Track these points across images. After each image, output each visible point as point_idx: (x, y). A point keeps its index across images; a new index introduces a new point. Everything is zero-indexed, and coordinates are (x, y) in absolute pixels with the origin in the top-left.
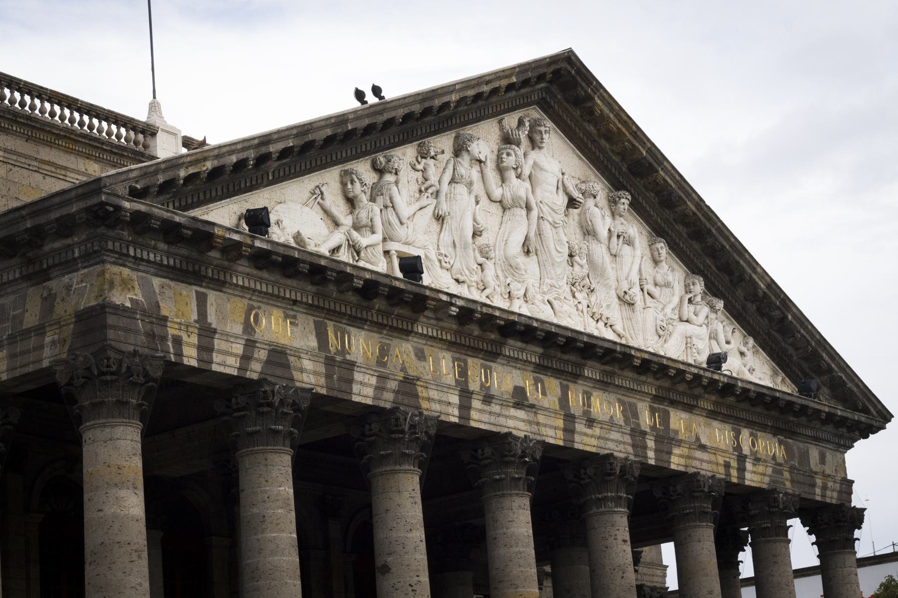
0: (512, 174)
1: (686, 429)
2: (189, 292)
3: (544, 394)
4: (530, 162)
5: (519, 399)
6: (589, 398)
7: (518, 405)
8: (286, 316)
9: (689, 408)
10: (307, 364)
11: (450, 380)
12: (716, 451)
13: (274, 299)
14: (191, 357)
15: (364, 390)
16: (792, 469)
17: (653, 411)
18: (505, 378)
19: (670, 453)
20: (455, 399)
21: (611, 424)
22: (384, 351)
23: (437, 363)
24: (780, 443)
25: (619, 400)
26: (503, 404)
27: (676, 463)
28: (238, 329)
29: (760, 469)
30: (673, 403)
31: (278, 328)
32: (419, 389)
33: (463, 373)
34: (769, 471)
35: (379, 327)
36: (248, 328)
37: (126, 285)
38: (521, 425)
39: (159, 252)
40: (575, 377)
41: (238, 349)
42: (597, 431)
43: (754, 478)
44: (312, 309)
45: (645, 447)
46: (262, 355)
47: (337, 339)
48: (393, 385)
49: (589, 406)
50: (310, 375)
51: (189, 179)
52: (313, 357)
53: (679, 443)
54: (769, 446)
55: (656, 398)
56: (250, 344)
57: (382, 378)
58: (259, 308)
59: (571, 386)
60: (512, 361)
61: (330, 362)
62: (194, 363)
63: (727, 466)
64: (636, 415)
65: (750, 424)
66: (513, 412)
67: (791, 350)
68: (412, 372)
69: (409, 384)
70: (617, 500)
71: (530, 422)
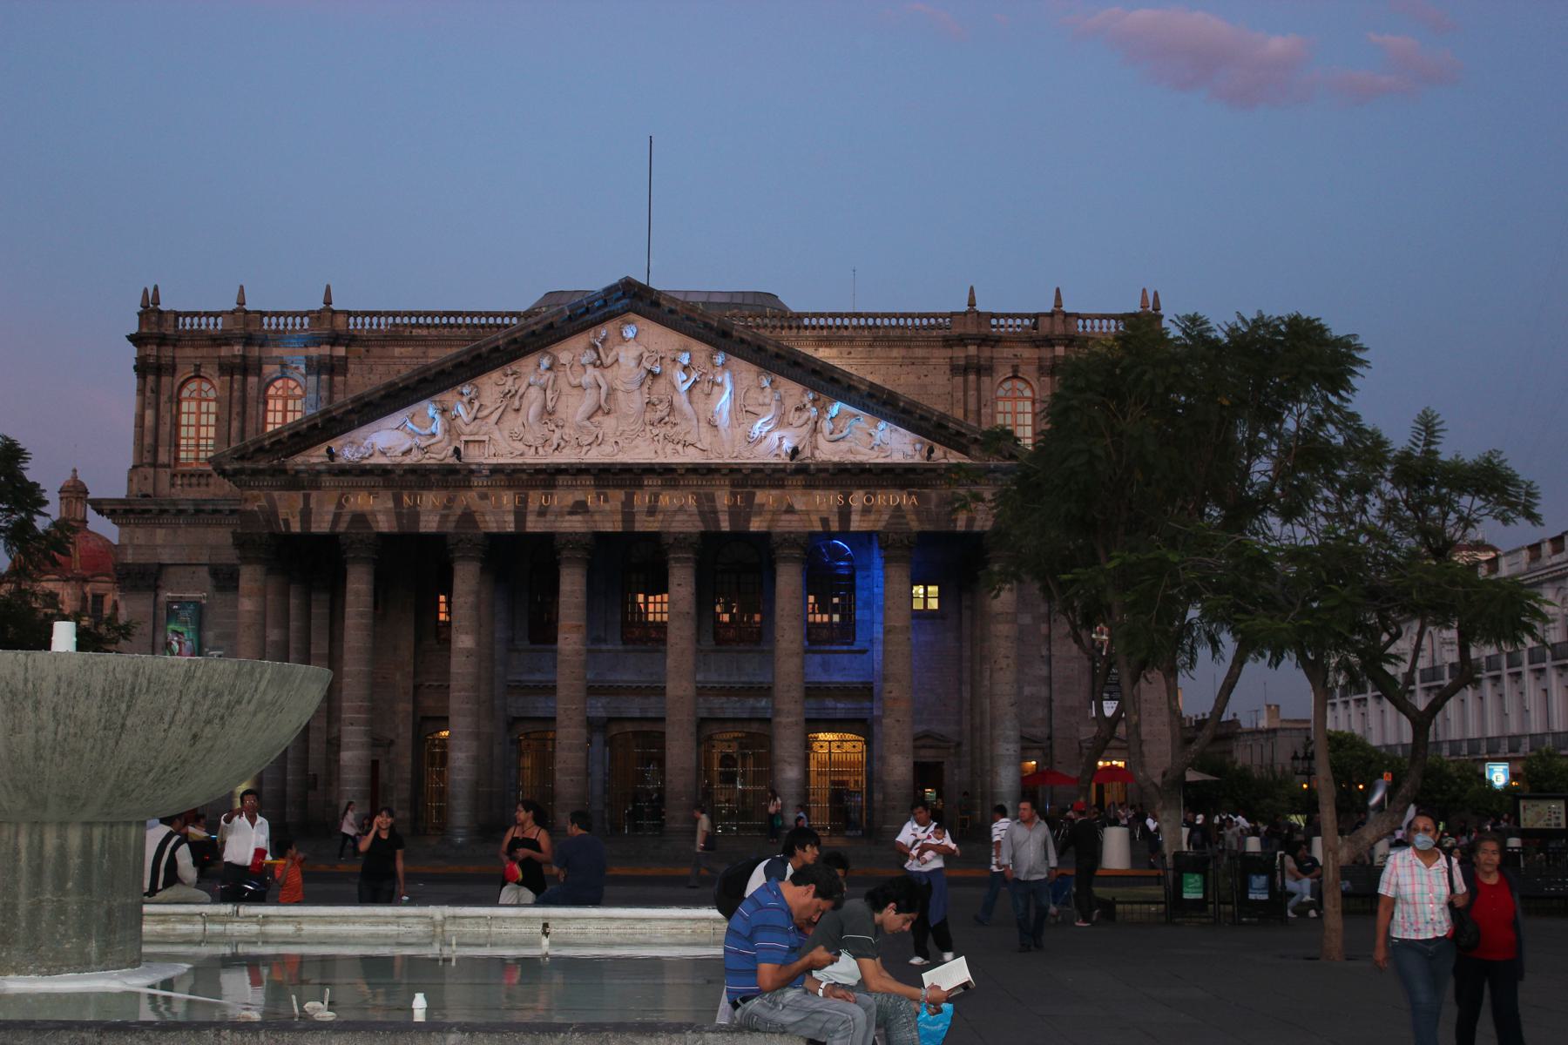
0: (590, 369)
2: (298, 497)
3: (606, 501)
4: (613, 354)
5: (580, 508)
6: (657, 496)
7: (571, 513)
9: (782, 486)
10: (381, 517)
11: (510, 507)
12: (808, 513)
13: (359, 487)
14: (296, 528)
15: (429, 523)
16: (917, 511)
17: (734, 495)
18: (563, 498)
19: (748, 521)
20: (511, 518)
21: (681, 509)
22: (450, 500)
23: (499, 499)
24: (910, 494)
26: (560, 514)
27: (756, 525)
28: (332, 508)
29: (873, 517)
30: (756, 486)
31: (361, 501)
33: (524, 501)
34: (886, 517)
35: (447, 487)
36: (340, 505)
37: (256, 498)
39: (268, 481)
40: (641, 486)
41: (329, 518)
42: (660, 517)
43: (856, 524)
44: (386, 487)
45: (717, 521)
46: (346, 518)
48: (452, 518)
49: (656, 501)
50: (384, 524)
51: (273, 444)
52: (386, 512)
53: (760, 514)
54: (888, 499)
55: (733, 485)
56: (337, 517)
57: (442, 516)
60: (568, 486)
61: (399, 516)
62: (298, 530)
63: (825, 521)
64: (711, 499)
65: (860, 487)
67: (923, 424)
69: (468, 517)
70: (678, 560)
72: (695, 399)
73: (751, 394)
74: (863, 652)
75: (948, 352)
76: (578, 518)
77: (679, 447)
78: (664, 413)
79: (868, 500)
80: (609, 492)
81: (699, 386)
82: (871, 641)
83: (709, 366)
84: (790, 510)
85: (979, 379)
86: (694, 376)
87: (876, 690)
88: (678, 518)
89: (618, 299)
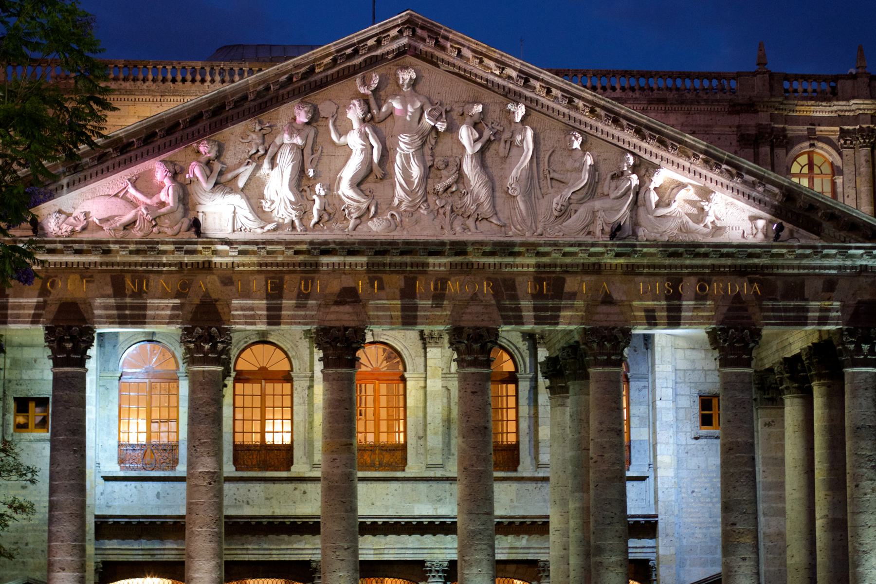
1: (589, 289)
3: (381, 287)
6: (442, 281)
7: (337, 303)
8: (82, 278)
21: (474, 298)
24: (751, 282)
25: (488, 279)
32: (219, 307)
38: (347, 317)
47: (134, 285)
58: (56, 276)
59: (420, 277)
66: (334, 308)
68: (214, 296)
71: (358, 315)
72: (489, 161)
73: (556, 157)
74: (643, 479)
75: (736, 120)
76: (347, 308)
77: (470, 223)
78: (450, 181)
79: (702, 288)
80: (386, 278)
81: (494, 146)
82: (653, 466)
83: (504, 122)
84: (608, 300)
85: (772, 151)
86: (487, 133)
87: (660, 526)
88: (468, 311)
89: (395, 38)
